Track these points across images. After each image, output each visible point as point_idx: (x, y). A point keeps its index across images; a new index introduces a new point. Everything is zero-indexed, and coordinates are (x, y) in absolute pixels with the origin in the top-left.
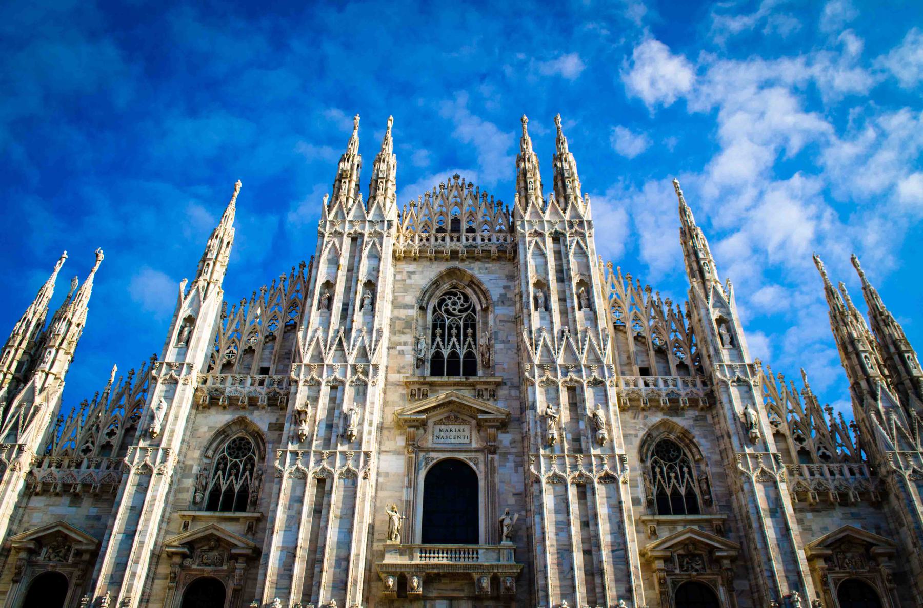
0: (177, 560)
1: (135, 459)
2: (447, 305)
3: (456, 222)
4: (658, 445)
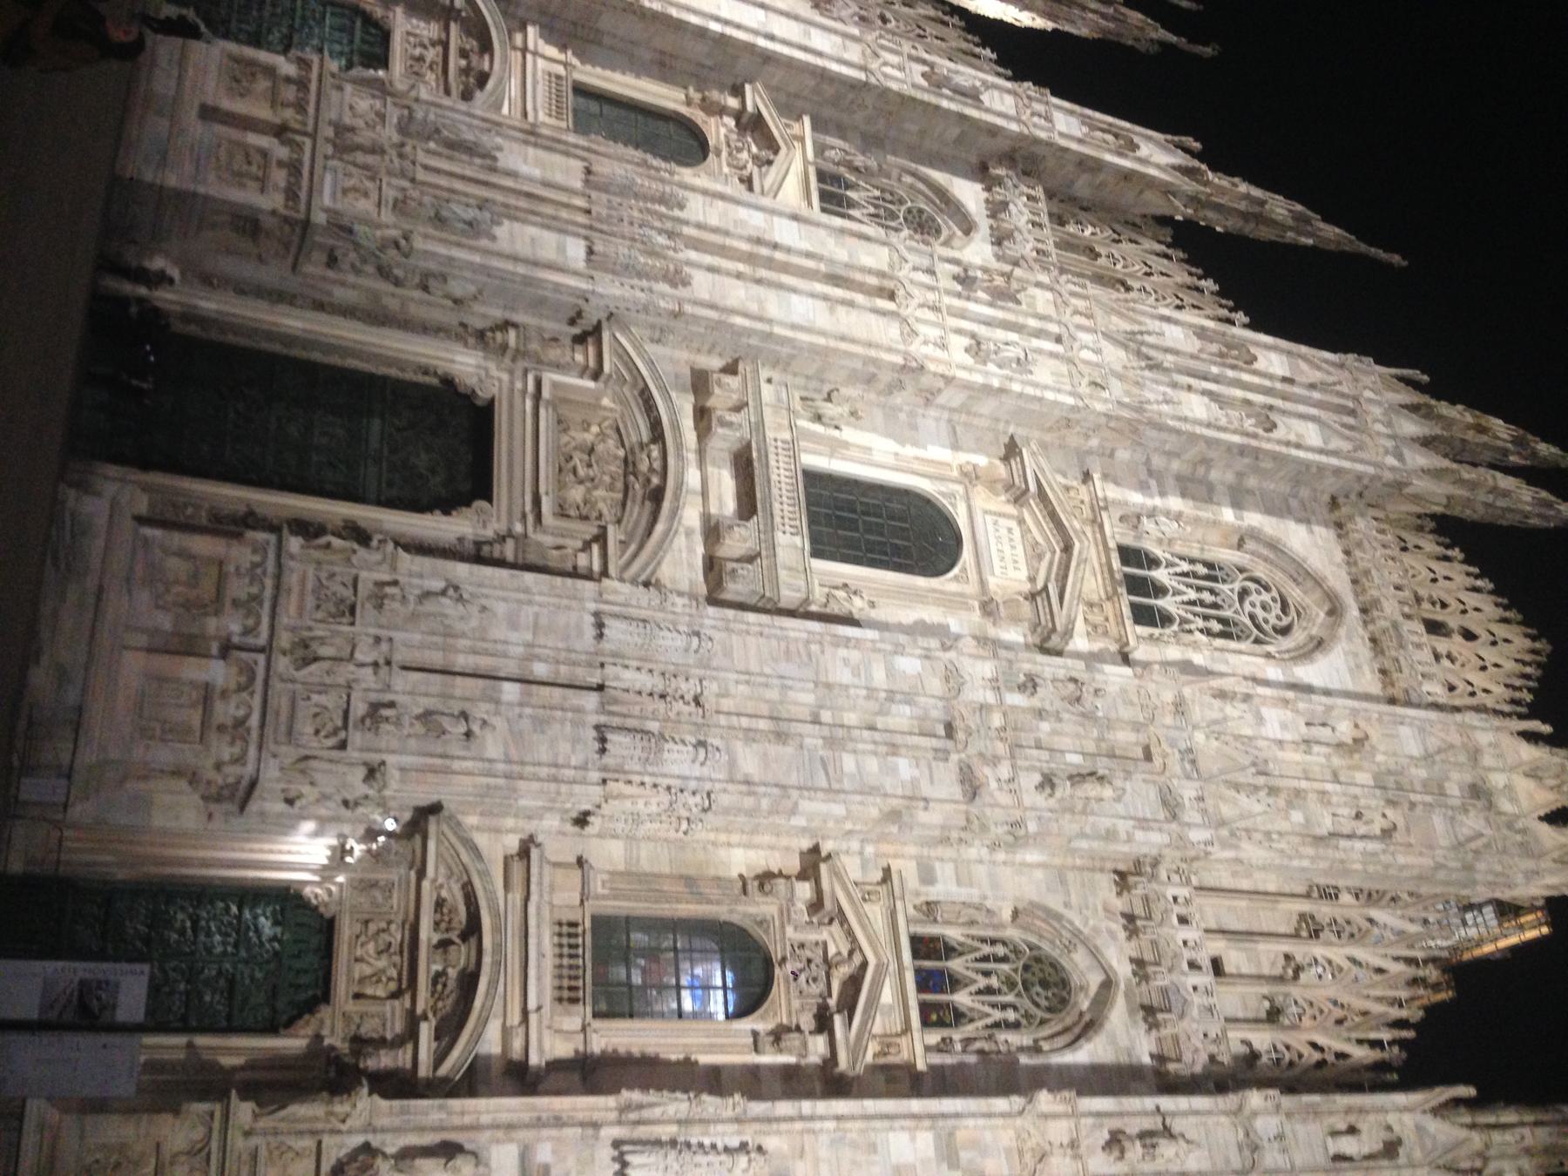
2: (1259, 593)
4: (1055, 965)
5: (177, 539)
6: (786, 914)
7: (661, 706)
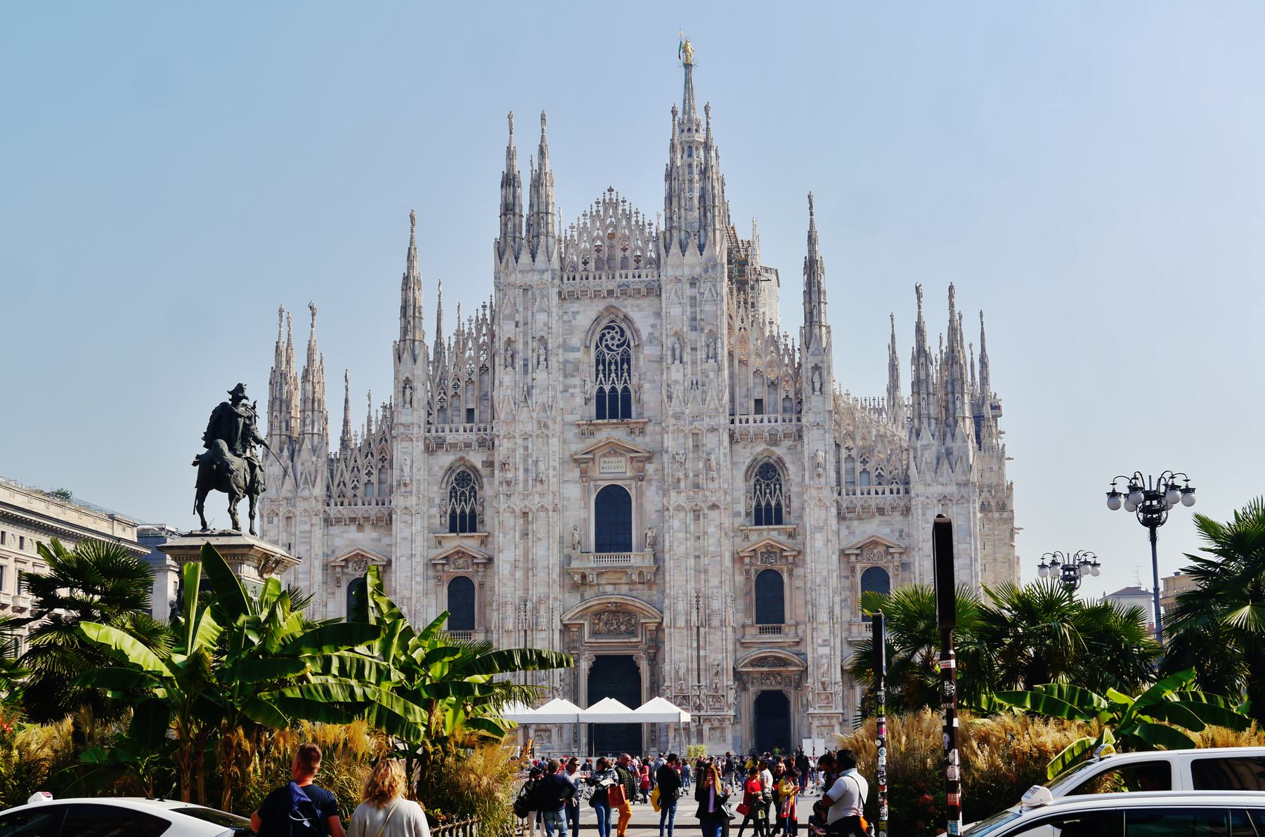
0: (439, 567)
1: (398, 501)
3: (611, 247)
4: (761, 467)
5: (671, 740)
6: (751, 565)
7: (701, 610)
